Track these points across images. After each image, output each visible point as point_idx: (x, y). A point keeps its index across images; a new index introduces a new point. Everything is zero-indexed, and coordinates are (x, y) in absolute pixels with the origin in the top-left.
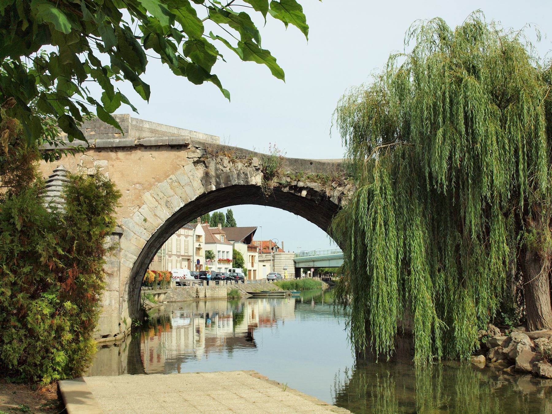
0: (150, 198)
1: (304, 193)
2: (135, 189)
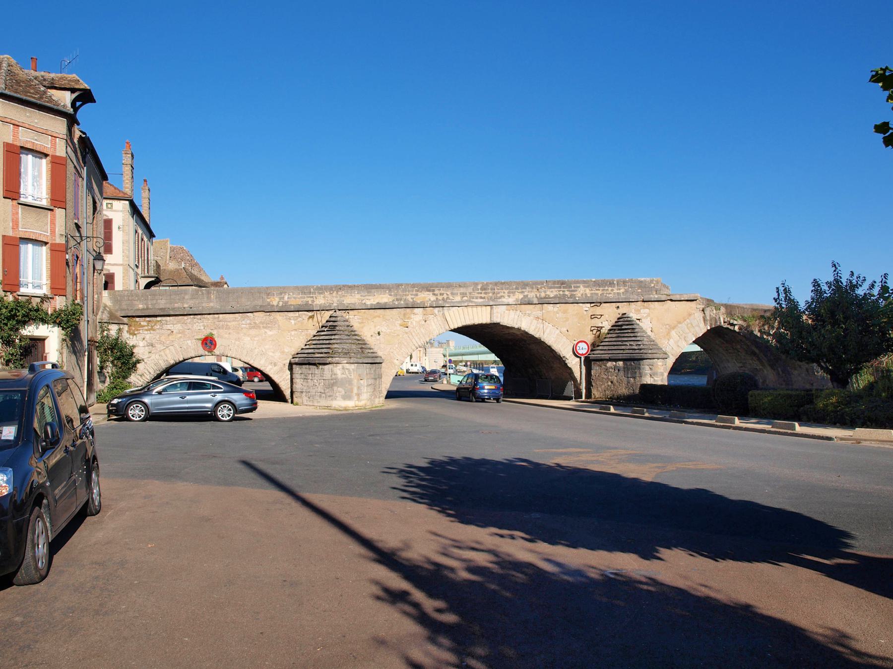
0: (675, 334)
1: (736, 328)
2: (666, 328)
